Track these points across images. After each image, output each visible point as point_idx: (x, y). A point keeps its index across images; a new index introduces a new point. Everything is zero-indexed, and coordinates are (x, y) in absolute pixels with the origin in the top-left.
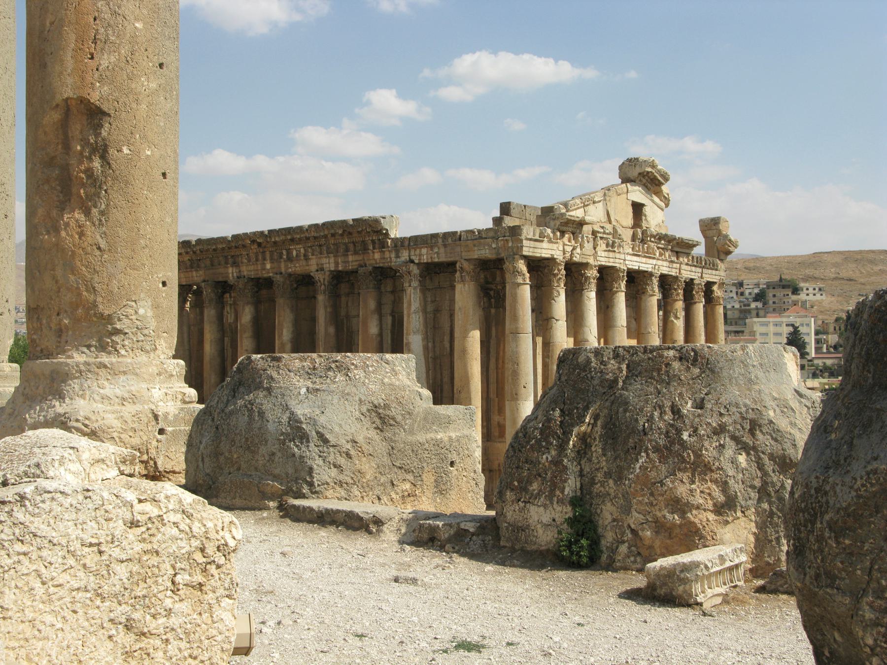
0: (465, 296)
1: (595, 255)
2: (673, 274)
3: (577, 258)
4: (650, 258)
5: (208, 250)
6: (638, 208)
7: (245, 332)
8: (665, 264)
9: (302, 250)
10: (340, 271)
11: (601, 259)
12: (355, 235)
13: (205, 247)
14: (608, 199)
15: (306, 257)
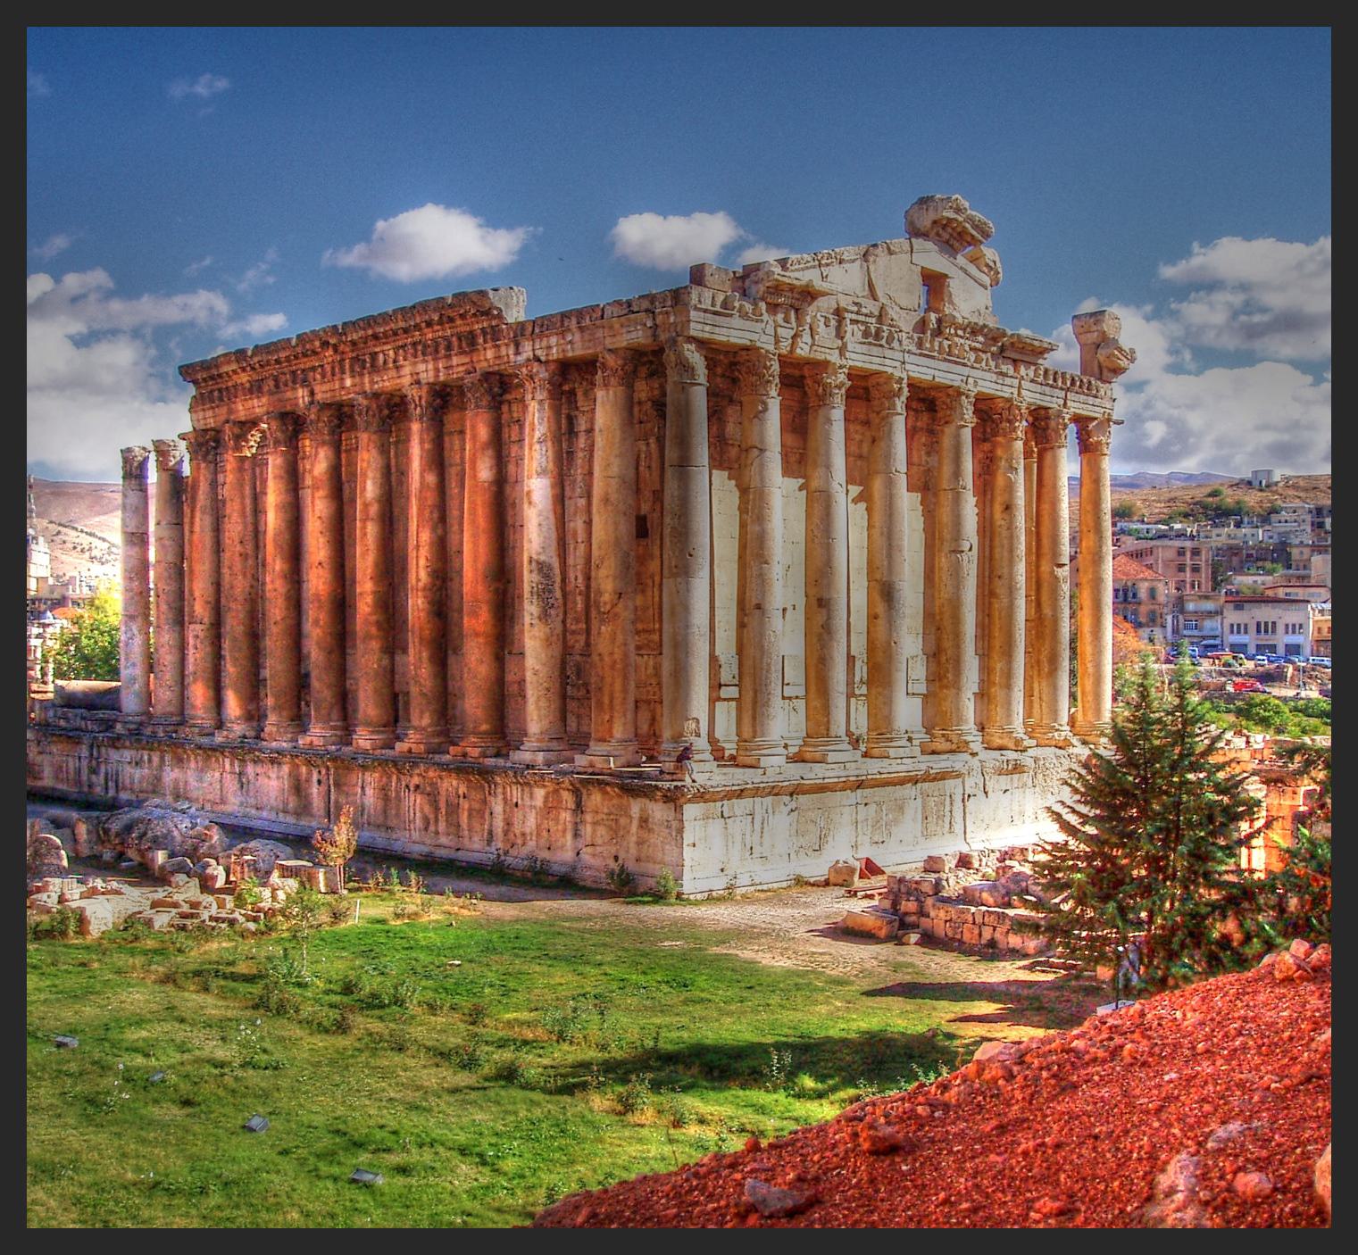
1: (842, 350)
2: (1007, 395)
3: (803, 350)
4: (956, 363)
5: (268, 363)
6: (934, 283)
8: (988, 376)
9: (391, 353)
10: (445, 385)
11: (854, 356)
12: (459, 322)
13: (265, 357)
14: (871, 259)
15: (398, 368)
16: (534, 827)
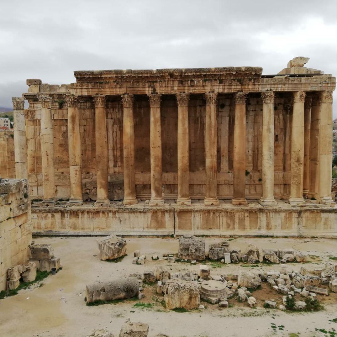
0: (299, 107)
7: (158, 122)
16: (280, 223)
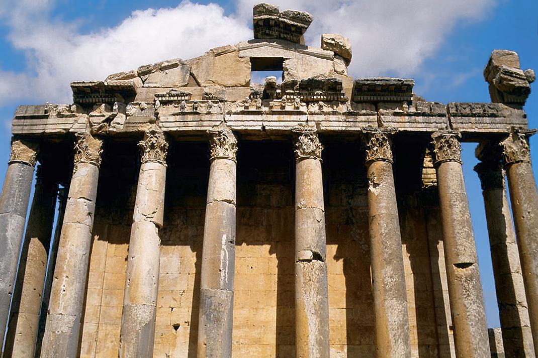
11: (168, 124)
